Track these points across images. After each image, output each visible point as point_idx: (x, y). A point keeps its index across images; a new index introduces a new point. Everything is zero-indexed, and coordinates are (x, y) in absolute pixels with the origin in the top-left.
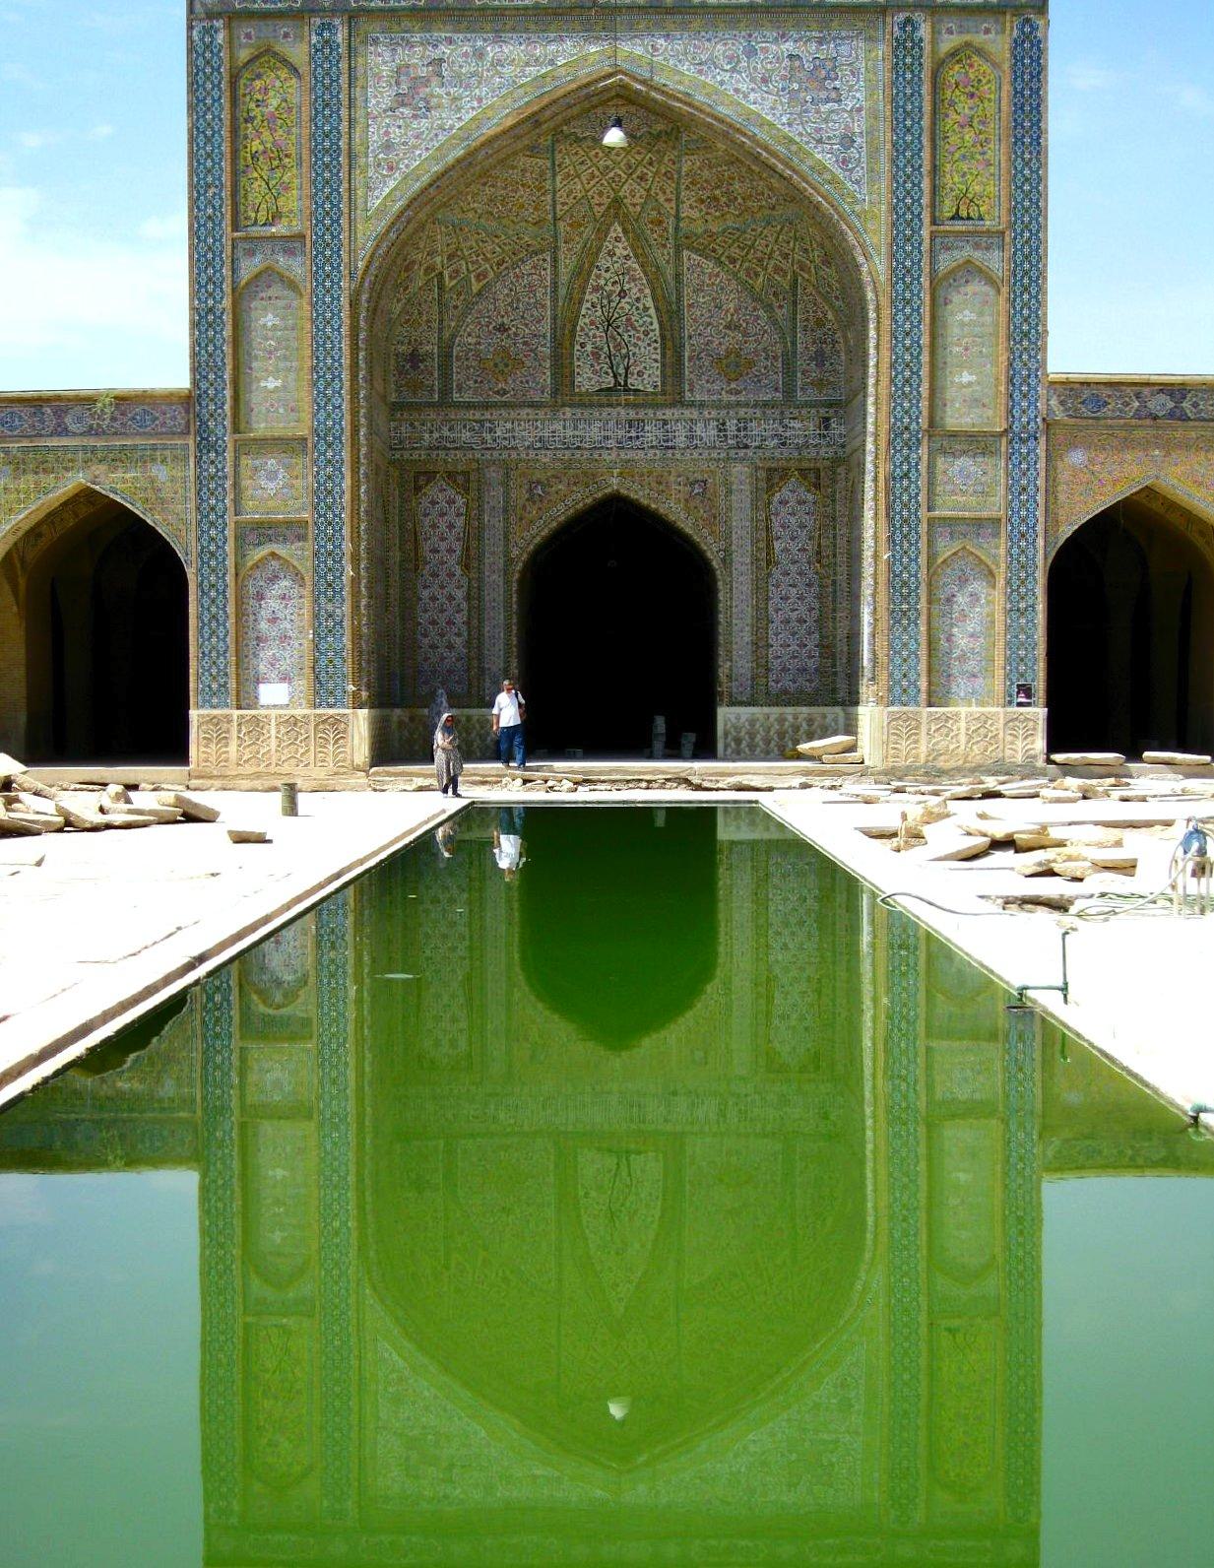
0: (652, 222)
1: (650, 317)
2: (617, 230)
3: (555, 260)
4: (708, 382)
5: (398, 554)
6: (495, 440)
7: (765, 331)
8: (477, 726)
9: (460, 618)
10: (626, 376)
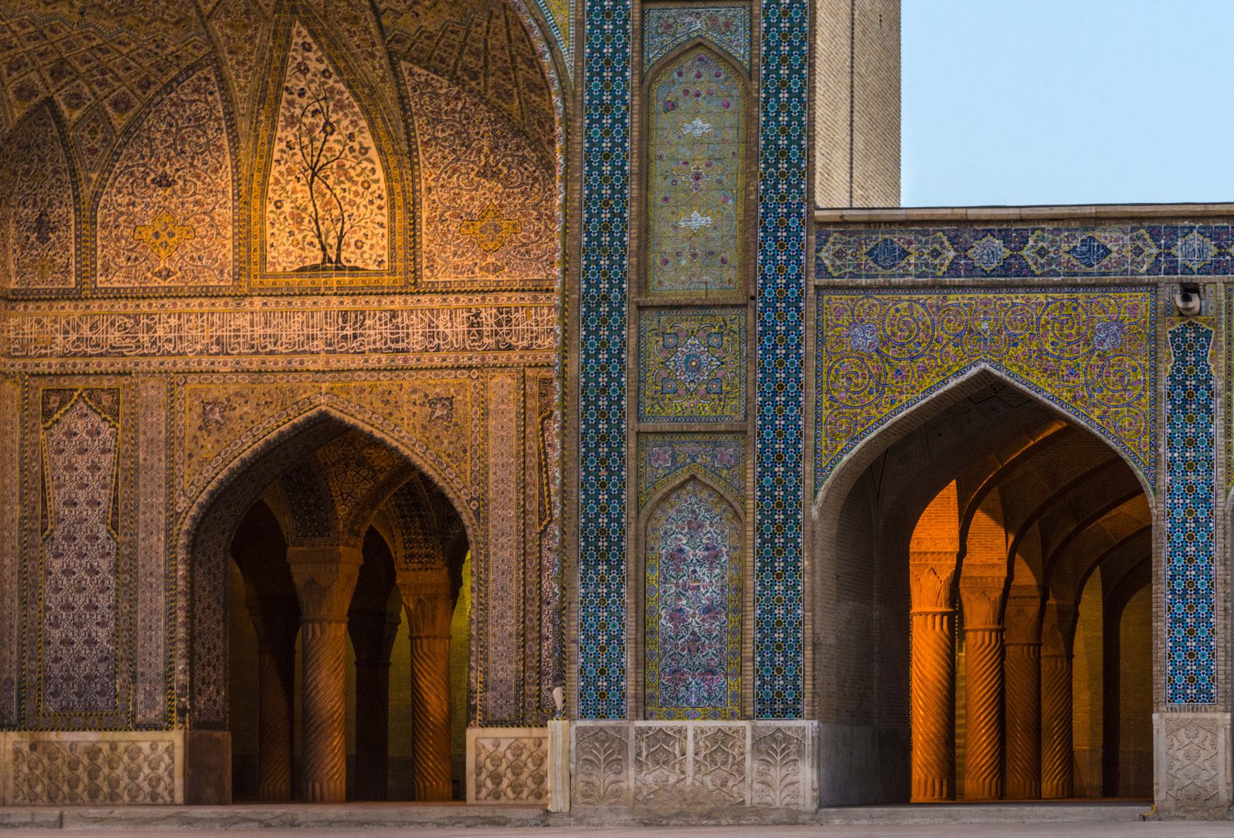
0: (345, 19)
1: (372, 161)
2: (300, 34)
3: (222, 79)
4: (455, 254)
5: (17, 507)
6: (154, 343)
7: (536, 180)
8: (126, 758)
9: (104, 601)
10: (339, 249)
